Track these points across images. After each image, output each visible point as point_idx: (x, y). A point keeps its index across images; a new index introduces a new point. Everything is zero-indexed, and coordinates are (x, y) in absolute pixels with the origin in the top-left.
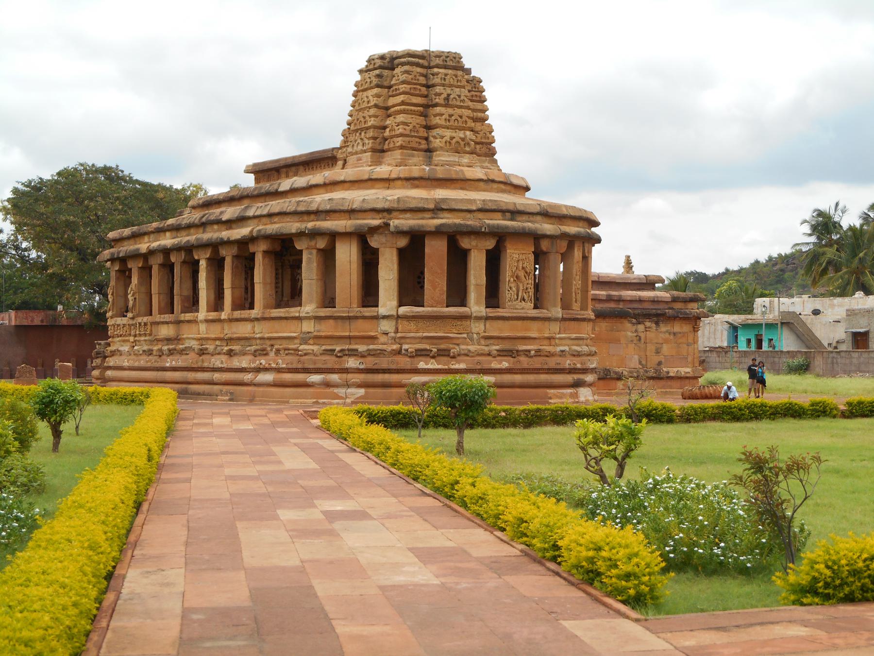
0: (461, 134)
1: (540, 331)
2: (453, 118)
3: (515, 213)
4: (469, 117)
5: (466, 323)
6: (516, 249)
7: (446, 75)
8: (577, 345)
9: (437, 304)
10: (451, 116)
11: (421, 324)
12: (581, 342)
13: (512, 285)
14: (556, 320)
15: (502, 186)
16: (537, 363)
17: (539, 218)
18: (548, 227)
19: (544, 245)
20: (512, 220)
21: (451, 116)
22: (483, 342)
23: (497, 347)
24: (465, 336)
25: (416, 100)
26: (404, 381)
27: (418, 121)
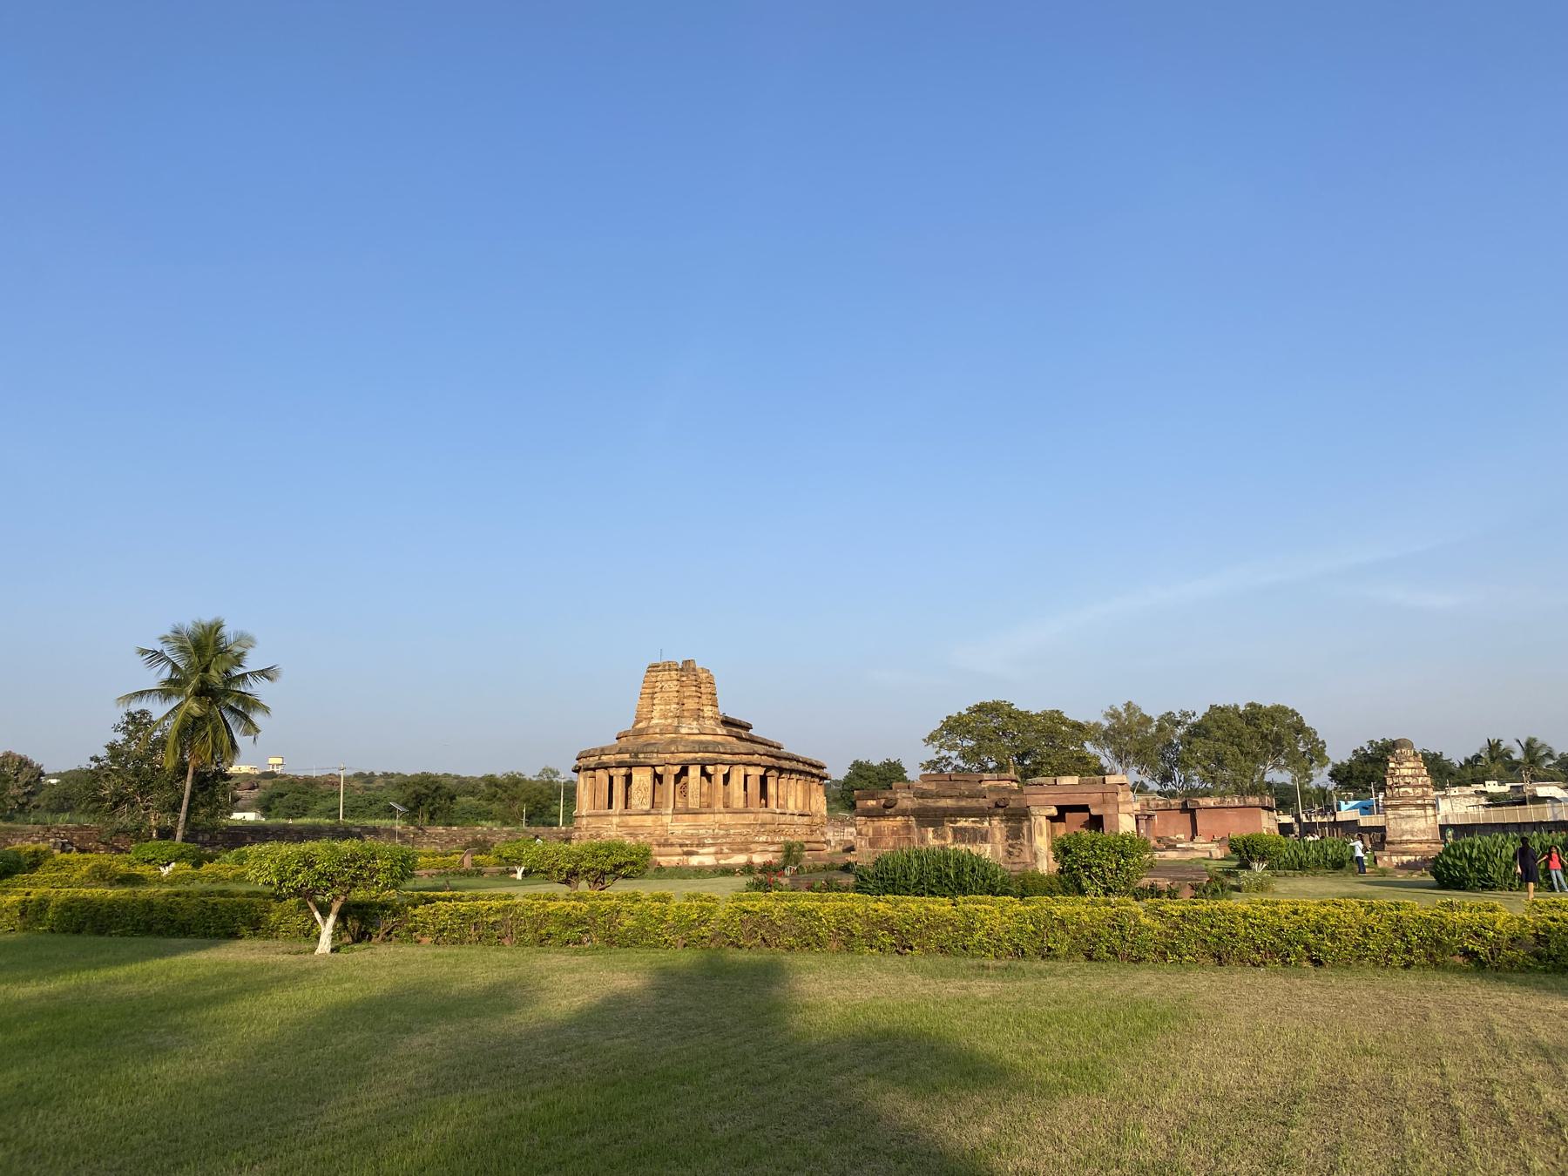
19: (659, 770)
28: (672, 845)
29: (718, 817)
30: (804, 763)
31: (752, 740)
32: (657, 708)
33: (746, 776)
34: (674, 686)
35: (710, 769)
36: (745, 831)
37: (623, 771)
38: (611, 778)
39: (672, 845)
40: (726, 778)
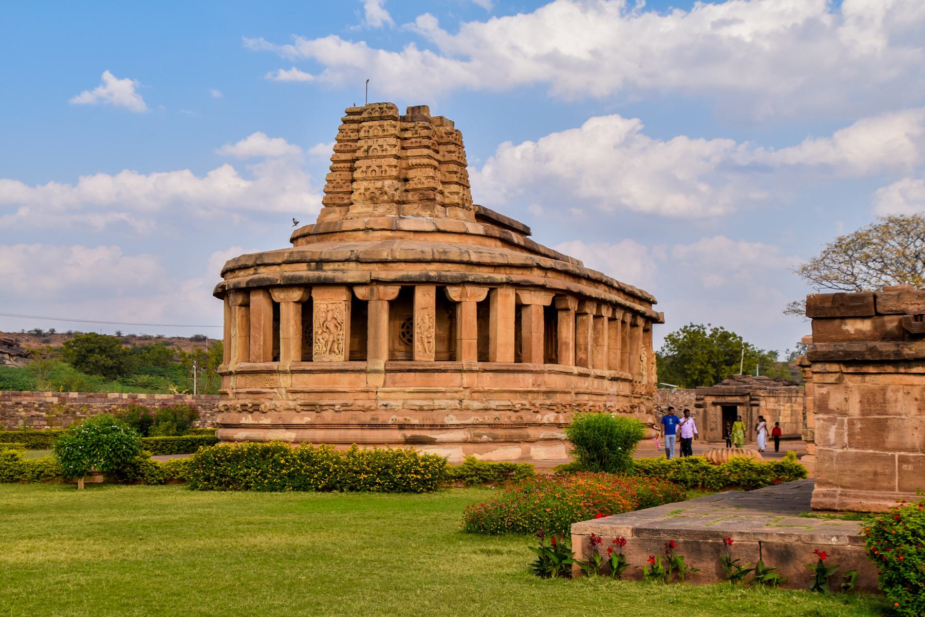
0: (379, 184)
1: (350, 383)
2: (371, 169)
3: (320, 263)
4: (389, 166)
5: (274, 377)
6: (322, 300)
7: (370, 127)
8: (426, 399)
9: (258, 358)
10: (368, 167)
11: (250, 378)
12: (433, 395)
13: (320, 337)
14: (376, 372)
15: (389, 234)
16: (343, 417)
17: (353, 265)
18: (353, 273)
19: (361, 293)
20: (317, 269)
21: (368, 167)
22: (291, 396)
23: (300, 402)
24: (275, 390)
25: (343, 157)
26: (236, 437)
27: (343, 177)
28: (385, 426)
29: (466, 379)
30: (621, 290)
31: (532, 249)
32: (359, 186)
33: (520, 307)
34: (390, 145)
35: (454, 293)
36: (518, 402)
37: (297, 295)
38: (276, 307)
39: (385, 426)
40: (484, 309)
